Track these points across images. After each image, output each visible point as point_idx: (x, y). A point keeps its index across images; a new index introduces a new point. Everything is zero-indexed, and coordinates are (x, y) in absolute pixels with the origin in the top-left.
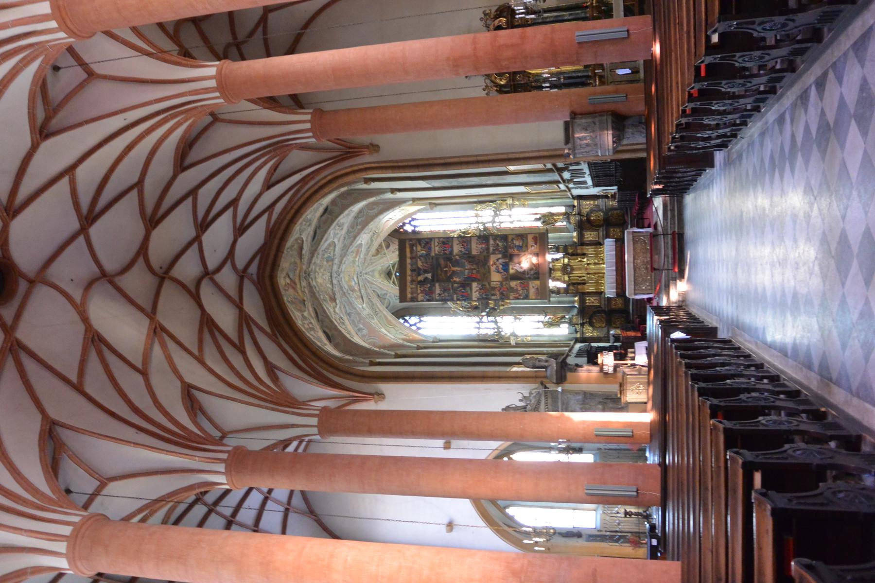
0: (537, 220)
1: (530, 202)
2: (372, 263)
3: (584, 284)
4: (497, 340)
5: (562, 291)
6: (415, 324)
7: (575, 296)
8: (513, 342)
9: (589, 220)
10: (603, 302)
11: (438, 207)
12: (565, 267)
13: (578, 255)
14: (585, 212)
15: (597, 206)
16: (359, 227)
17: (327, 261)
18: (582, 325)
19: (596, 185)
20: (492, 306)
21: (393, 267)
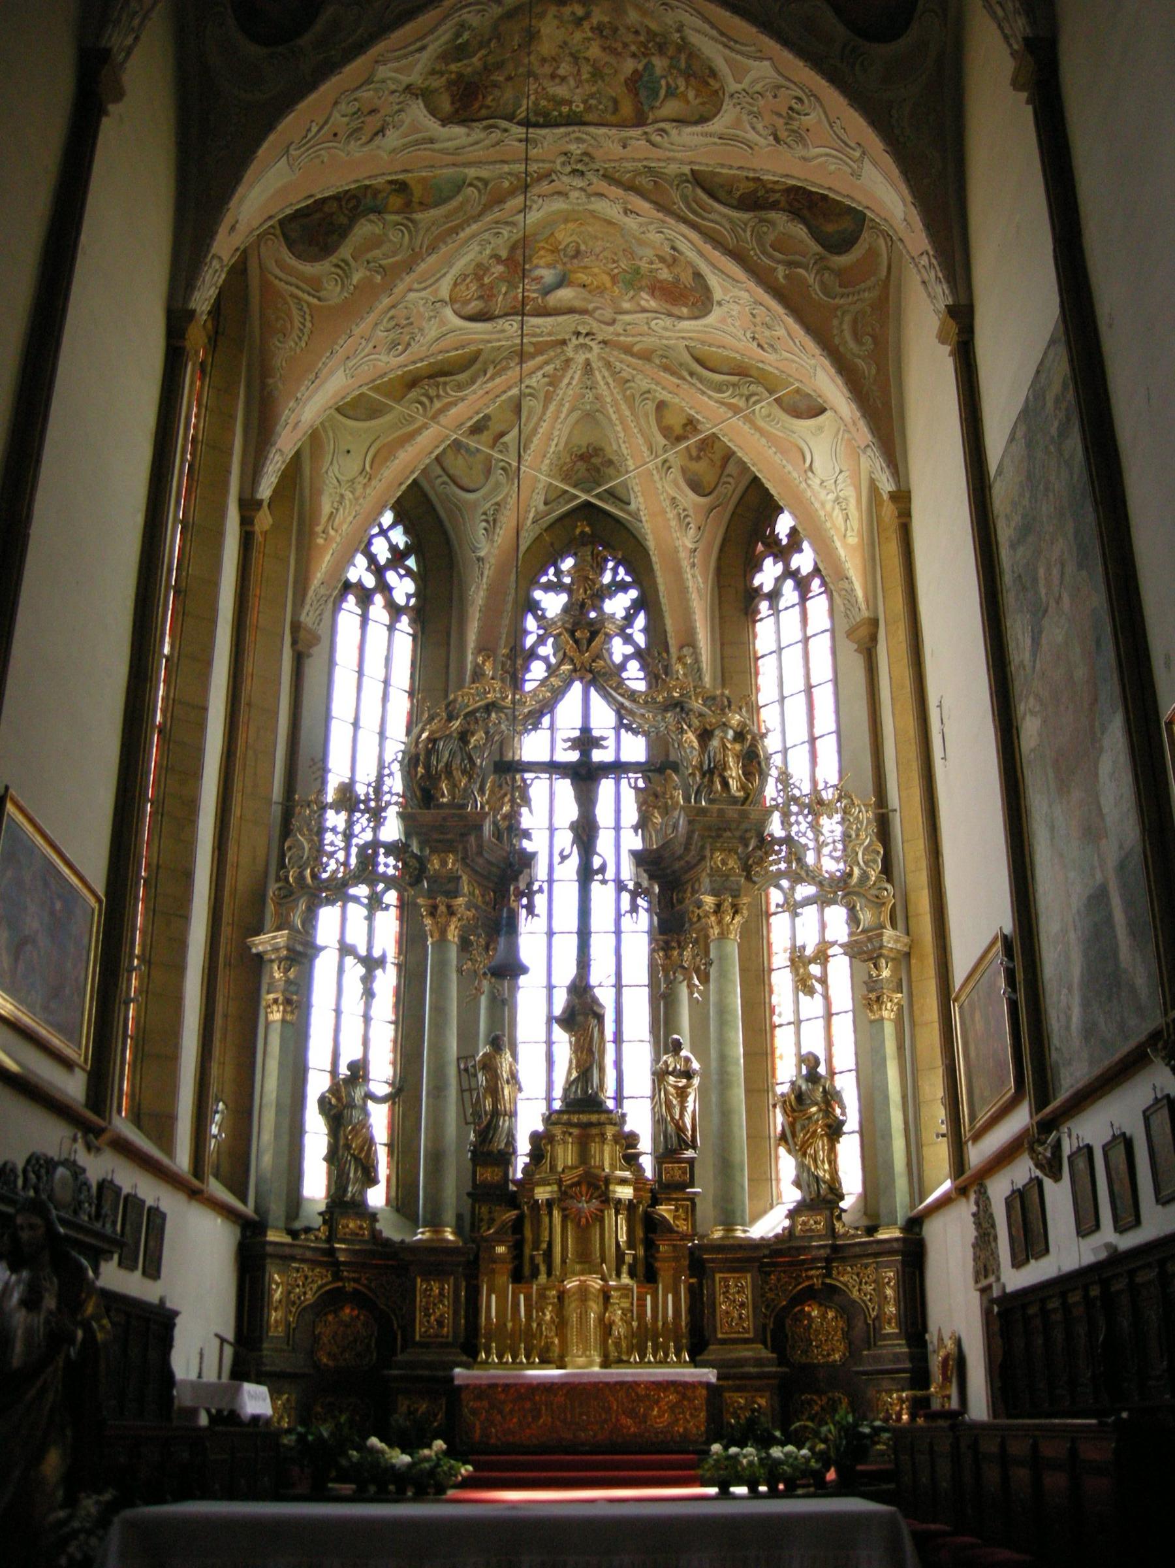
1: (889, 1029)
2: (630, 401)
3: (517, 1277)
4: (279, 884)
5: (489, 1175)
7: (458, 1231)
8: (263, 943)
9: (810, 1295)
10: (428, 1357)
12: (598, 1186)
13: (650, 1245)
14: (845, 1278)
15: (873, 1334)
16: (781, 272)
17: (634, 83)
19: (1007, 1316)
20: (435, 864)
21: (612, 495)
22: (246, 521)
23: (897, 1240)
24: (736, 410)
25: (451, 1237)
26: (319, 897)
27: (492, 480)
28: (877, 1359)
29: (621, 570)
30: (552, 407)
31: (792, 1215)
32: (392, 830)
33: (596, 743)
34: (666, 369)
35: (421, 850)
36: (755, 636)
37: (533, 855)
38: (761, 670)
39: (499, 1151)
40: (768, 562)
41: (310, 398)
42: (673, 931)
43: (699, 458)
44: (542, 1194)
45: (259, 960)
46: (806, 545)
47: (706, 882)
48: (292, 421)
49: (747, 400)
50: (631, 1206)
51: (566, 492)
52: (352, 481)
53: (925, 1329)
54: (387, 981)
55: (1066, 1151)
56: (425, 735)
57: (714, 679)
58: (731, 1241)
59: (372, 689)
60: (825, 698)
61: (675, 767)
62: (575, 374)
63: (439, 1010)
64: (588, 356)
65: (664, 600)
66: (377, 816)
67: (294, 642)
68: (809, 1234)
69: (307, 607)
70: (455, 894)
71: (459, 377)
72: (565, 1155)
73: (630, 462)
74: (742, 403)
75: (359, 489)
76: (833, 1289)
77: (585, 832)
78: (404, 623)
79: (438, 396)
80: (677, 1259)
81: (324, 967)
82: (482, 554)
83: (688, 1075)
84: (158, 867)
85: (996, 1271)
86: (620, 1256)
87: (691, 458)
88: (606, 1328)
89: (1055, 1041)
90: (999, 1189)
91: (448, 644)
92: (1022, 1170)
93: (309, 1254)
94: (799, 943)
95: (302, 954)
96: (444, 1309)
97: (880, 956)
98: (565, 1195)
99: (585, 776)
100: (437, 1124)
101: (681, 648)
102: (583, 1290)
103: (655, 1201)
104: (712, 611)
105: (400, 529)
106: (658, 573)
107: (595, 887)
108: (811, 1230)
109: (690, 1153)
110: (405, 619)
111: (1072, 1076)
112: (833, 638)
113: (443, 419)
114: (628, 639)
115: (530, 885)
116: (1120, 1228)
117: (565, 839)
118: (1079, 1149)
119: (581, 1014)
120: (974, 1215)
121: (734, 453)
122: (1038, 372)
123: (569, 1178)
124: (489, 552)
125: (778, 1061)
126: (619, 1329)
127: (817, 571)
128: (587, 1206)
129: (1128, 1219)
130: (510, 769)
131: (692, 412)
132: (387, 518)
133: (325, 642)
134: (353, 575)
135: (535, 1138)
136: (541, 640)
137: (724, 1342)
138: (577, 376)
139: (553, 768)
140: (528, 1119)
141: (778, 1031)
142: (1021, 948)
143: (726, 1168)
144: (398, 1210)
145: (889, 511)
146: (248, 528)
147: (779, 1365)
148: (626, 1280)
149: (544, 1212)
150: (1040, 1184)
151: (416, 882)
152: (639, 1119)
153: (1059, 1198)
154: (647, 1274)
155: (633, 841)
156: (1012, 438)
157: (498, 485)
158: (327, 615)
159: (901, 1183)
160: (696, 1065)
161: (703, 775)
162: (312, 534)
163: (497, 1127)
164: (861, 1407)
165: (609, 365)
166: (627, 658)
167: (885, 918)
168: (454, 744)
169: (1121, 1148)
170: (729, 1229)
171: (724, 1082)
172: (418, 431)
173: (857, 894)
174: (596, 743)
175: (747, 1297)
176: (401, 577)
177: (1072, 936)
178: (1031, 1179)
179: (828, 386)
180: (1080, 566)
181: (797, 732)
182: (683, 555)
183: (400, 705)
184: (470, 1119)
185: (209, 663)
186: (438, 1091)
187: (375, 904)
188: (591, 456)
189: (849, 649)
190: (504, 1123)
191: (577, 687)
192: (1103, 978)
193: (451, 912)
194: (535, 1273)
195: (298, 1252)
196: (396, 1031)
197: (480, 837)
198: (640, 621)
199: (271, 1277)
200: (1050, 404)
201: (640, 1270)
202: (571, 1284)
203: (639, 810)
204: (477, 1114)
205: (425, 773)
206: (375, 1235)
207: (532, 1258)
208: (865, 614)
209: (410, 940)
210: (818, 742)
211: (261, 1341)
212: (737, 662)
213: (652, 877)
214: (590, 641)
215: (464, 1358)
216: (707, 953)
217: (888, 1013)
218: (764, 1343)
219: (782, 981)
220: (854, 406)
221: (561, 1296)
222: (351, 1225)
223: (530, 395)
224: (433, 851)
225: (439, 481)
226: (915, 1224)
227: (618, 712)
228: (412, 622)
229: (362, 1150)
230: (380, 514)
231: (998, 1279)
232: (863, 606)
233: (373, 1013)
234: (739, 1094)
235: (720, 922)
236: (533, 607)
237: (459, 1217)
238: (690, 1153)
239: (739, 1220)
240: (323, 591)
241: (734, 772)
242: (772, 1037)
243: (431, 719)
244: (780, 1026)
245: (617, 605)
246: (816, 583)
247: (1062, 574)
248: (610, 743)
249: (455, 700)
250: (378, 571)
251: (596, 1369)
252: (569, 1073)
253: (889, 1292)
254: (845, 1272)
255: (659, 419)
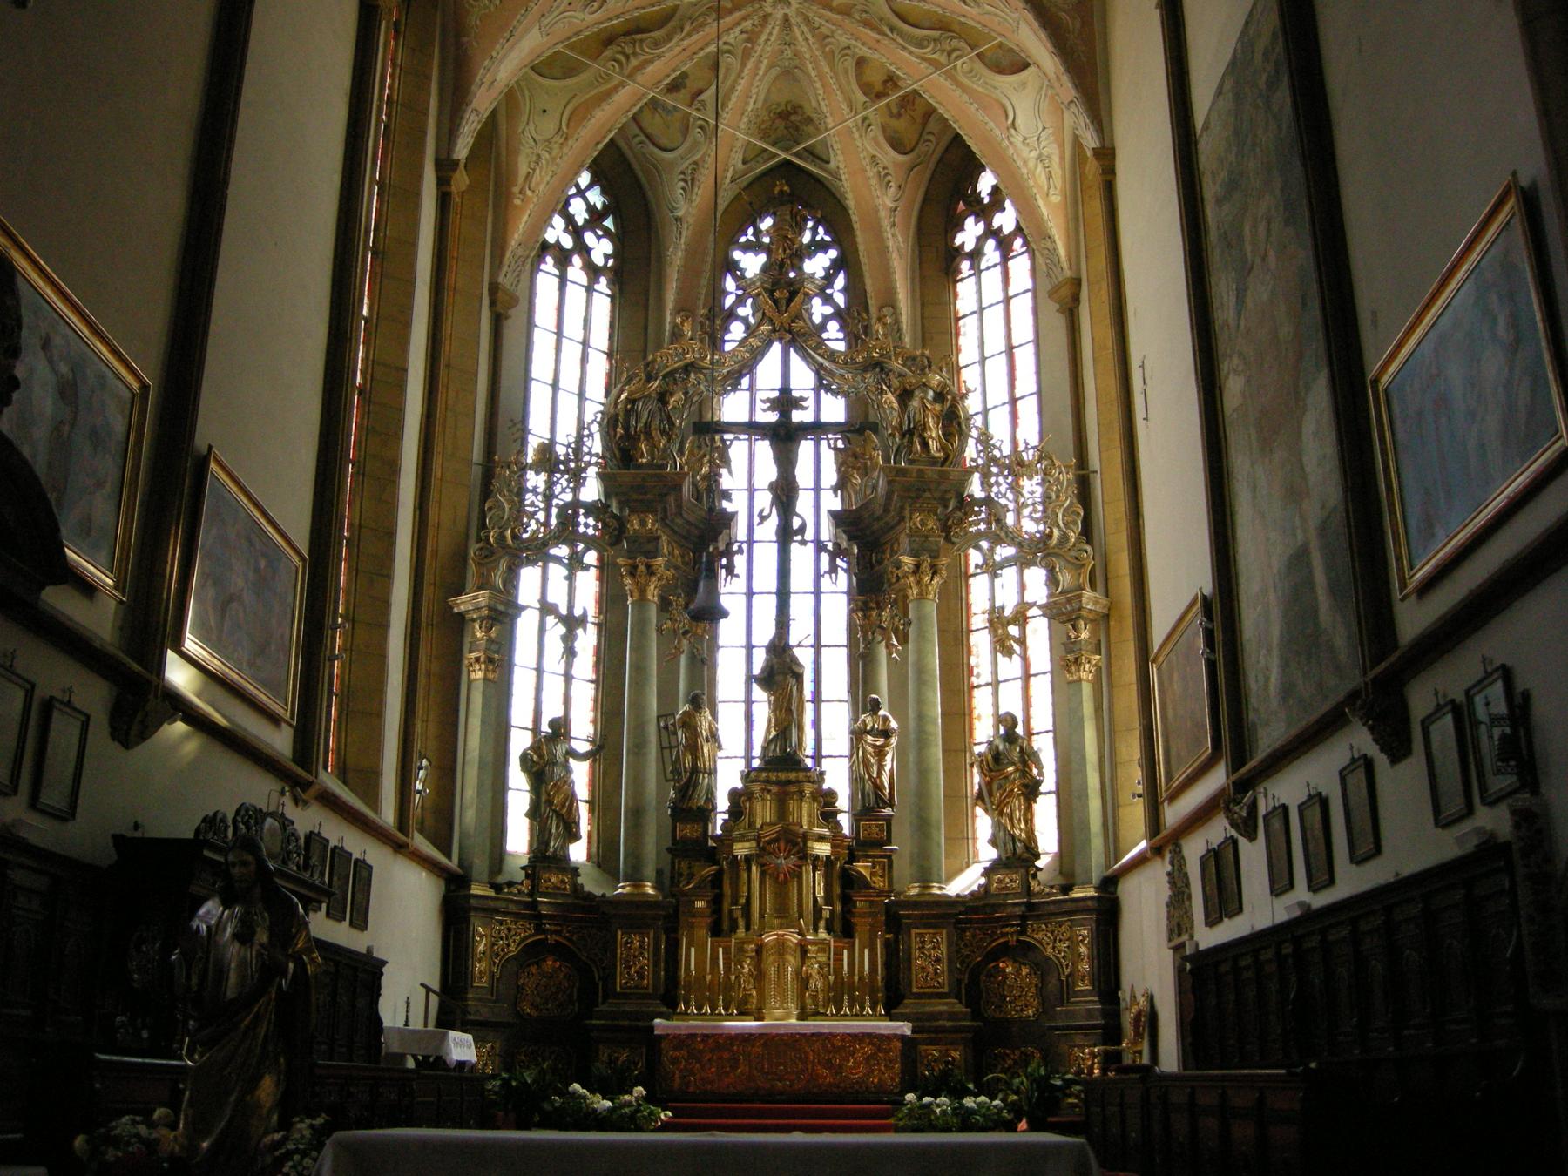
0: (1006, 722)
1: (1087, 690)
2: (830, 57)
3: (716, 931)
5: (689, 831)
6: (583, 249)
8: (464, 603)
9: (1004, 951)
11: (1059, 323)
12: (795, 842)
13: (847, 901)
14: (1040, 935)
15: (1066, 991)
18: (530, 912)
19: (1200, 974)
20: (634, 524)
21: (811, 153)
22: (443, 182)
23: (1091, 898)
24: (937, 66)
25: (651, 892)
26: (520, 557)
27: (689, 140)
28: (1070, 1015)
29: (821, 230)
30: (750, 65)
31: (987, 873)
32: (591, 491)
33: (797, 403)
34: (866, 24)
35: (621, 510)
36: (956, 296)
37: (733, 515)
38: (962, 330)
39: (699, 808)
40: (970, 221)
41: (505, 56)
42: (873, 593)
43: (899, 115)
44: (741, 849)
45: (461, 621)
46: (1008, 204)
47: (905, 541)
48: (487, 80)
49: (949, 55)
50: (829, 862)
51: (765, 150)
52: (549, 141)
53: (1118, 986)
54: (587, 640)
55: (1262, 811)
56: (623, 396)
57: (914, 339)
58: (927, 898)
59: (571, 351)
60: (1026, 359)
61: (875, 428)
62: (773, 31)
63: (640, 669)
64: (787, 11)
65: (864, 259)
66: (577, 478)
67: (493, 304)
68: (1005, 892)
69: (505, 269)
70: (654, 554)
71: (656, 34)
72: (764, 812)
73: (830, 121)
74: (943, 59)
75: (556, 147)
76: (1028, 947)
77: (785, 493)
78: (602, 284)
79: (635, 54)
80: (873, 915)
81: (526, 626)
82: (680, 214)
83: (886, 734)
84: (360, 526)
85: (1190, 929)
86: (817, 911)
87: (891, 115)
88: (803, 981)
89: (1253, 701)
90: (1194, 849)
91: (646, 306)
92: (1218, 830)
93: (512, 908)
94: (998, 604)
95: (503, 614)
96: (645, 961)
97: (1078, 617)
98: (762, 850)
99: (785, 437)
100: (638, 781)
101: (880, 308)
102: (781, 945)
103: (852, 858)
104: (913, 271)
105: (597, 189)
106: (858, 233)
107: (795, 548)
108: (1006, 888)
109: (887, 811)
110: (603, 280)
111: (1269, 736)
112: (1035, 298)
113: (639, 78)
114: (828, 300)
115: (729, 544)
116: (1314, 887)
117: (764, 500)
118: (1275, 808)
119: (780, 673)
120: (1169, 874)
121: (934, 110)
122: (1247, 23)
123: (769, 834)
124: (687, 212)
125: (976, 722)
126: (816, 983)
127: (1019, 230)
128: (785, 862)
129: (1322, 877)
130: (710, 431)
131: (892, 68)
132: (584, 179)
133: (523, 304)
134: (550, 236)
135: (734, 795)
136: (740, 301)
137: (919, 996)
138: (775, 32)
139: (752, 429)
140: (728, 777)
141: (976, 692)
142: (1220, 609)
143: (923, 826)
144: (599, 866)
145: (1093, 168)
146: (445, 189)
147: (973, 1020)
148: (823, 934)
149: (743, 867)
150: (1235, 843)
151: (616, 541)
152: (837, 778)
153: (1253, 857)
154: (844, 929)
155: (832, 502)
156: (1219, 92)
157: (695, 145)
158: (525, 276)
159: (1097, 843)
160: (894, 724)
161: (903, 436)
162: (509, 196)
163: (696, 783)
164: (1053, 1060)
165: (807, 20)
166: (826, 319)
167: (1084, 579)
168: (653, 405)
169: (1317, 809)
170: (926, 885)
171: (922, 742)
172: (615, 89)
173: (1056, 555)
174: (797, 403)
175: (943, 952)
176: (599, 238)
177: (1272, 596)
178: (1226, 839)
179: (1032, 40)
180: (1287, 223)
181: (998, 392)
182: (883, 214)
183: (599, 367)
184: (670, 776)
185: (407, 325)
186: (638, 748)
187: (575, 564)
188: (790, 114)
189: (1051, 308)
190: (703, 780)
191: (776, 348)
192: (1302, 638)
193: (651, 571)
194: (734, 928)
195: (499, 904)
196: (597, 690)
197: (679, 498)
198: (840, 282)
199: (475, 932)
200: (1258, 57)
201: (837, 926)
202: (769, 938)
203: (839, 471)
204: (677, 771)
205: (624, 431)
206: (577, 889)
207: (731, 911)
208: (1068, 273)
209: (610, 600)
210: (1019, 404)
211: (465, 991)
212: (938, 325)
213: (850, 539)
214: (790, 300)
215: (664, 1009)
216: (906, 613)
217: (1086, 674)
218: (958, 997)
219: (981, 642)
220: (1057, 61)
221: (759, 950)
222: (553, 880)
223: (728, 51)
224: (632, 511)
225: (637, 140)
226: (1109, 884)
227: (817, 373)
228: (611, 283)
229: (563, 806)
230: (578, 173)
231: (1192, 937)
232: (1065, 265)
233: (574, 672)
234: (937, 753)
235: (918, 583)
236: (732, 267)
237: (659, 873)
238: (887, 811)
239: (935, 877)
240: (520, 252)
241: (934, 432)
242: (971, 697)
243: (630, 379)
244: (979, 686)
245: (817, 265)
246: (1018, 243)
247: (1269, 231)
248: (810, 403)
249: (654, 361)
250: (576, 231)
251: (794, 1021)
252: (768, 731)
253: (1083, 950)
254: (1039, 930)
255: (859, 75)
